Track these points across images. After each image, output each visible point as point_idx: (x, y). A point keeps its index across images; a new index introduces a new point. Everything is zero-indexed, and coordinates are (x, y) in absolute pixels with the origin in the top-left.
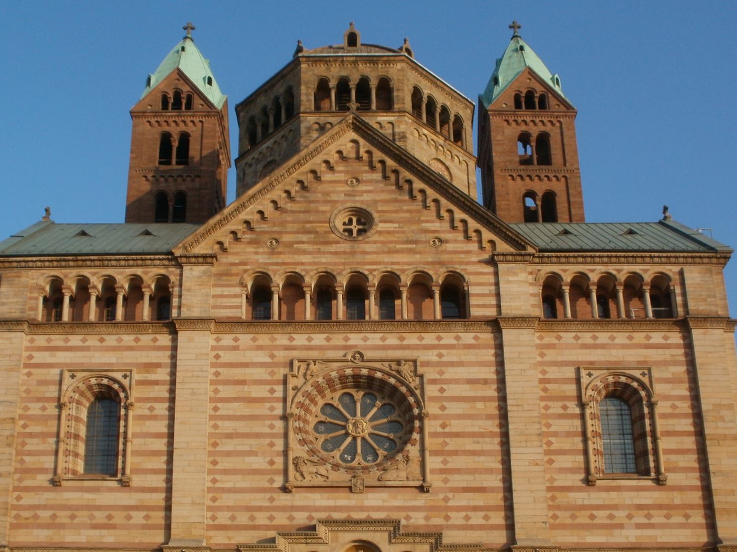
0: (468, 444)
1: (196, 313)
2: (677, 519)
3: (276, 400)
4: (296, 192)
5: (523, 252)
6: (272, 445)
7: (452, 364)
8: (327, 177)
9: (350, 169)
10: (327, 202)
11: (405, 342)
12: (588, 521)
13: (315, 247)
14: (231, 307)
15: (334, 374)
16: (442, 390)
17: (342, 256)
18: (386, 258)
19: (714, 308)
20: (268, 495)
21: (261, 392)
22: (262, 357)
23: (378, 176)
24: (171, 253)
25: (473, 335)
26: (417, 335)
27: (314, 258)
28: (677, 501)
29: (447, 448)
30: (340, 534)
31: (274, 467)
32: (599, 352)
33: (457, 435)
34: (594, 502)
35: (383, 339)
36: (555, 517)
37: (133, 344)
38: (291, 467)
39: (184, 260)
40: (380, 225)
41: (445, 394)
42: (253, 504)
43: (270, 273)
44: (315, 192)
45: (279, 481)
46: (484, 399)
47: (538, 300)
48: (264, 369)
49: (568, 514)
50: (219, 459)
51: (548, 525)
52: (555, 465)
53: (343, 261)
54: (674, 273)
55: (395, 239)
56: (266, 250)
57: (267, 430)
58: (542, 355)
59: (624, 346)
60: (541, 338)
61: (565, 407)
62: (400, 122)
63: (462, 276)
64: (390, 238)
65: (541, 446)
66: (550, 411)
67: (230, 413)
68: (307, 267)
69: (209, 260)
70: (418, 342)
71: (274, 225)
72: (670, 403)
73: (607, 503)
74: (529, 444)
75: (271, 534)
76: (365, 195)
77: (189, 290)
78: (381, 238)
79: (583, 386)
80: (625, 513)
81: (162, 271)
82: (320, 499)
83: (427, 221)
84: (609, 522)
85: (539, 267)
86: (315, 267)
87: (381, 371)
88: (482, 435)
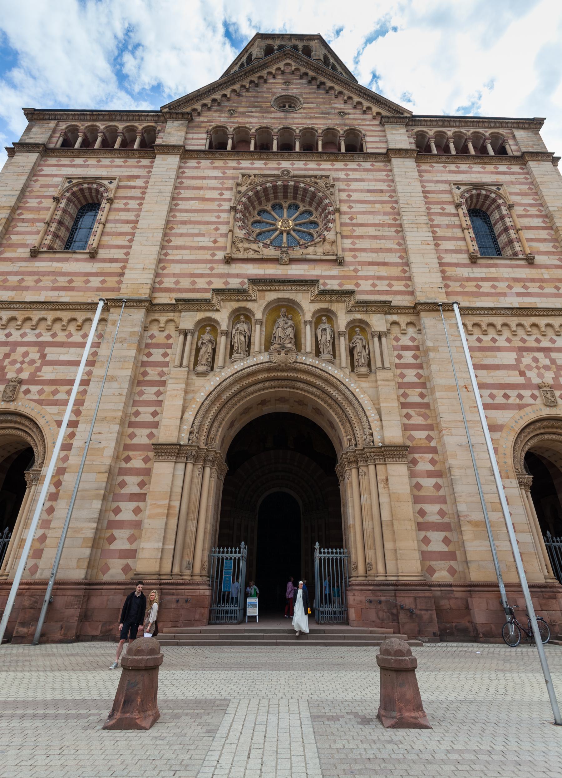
0: (371, 231)
3: (225, 200)
6: (217, 229)
7: (357, 180)
11: (321, 167)
12: (475, 290)
14: (198, 145)
15: (269, 185)
18: (308, 121)
20: (209, 266)
25: (370, 163)
26: (330, 163)
29: (354, 234)
30: (267, 294)
31: (217, 245)
32: (462, 175)
33: (362, 225)
39: (168, 116)
41: (351, 199)
42: (197, 272)
45: (220, 255)
46: (382, 202)
49: (458, 284)
52: (441, 247)
59: (479, 173)
64: (311, 111)
66: (431, 211)
67: (187, 207)
69: (186, 117)
70: (331, 167)
73: (488, 276)
74: (419, 230)
75: (208, 295)
78: (305, 111)
80: (507, 284)
88: (382, 225)
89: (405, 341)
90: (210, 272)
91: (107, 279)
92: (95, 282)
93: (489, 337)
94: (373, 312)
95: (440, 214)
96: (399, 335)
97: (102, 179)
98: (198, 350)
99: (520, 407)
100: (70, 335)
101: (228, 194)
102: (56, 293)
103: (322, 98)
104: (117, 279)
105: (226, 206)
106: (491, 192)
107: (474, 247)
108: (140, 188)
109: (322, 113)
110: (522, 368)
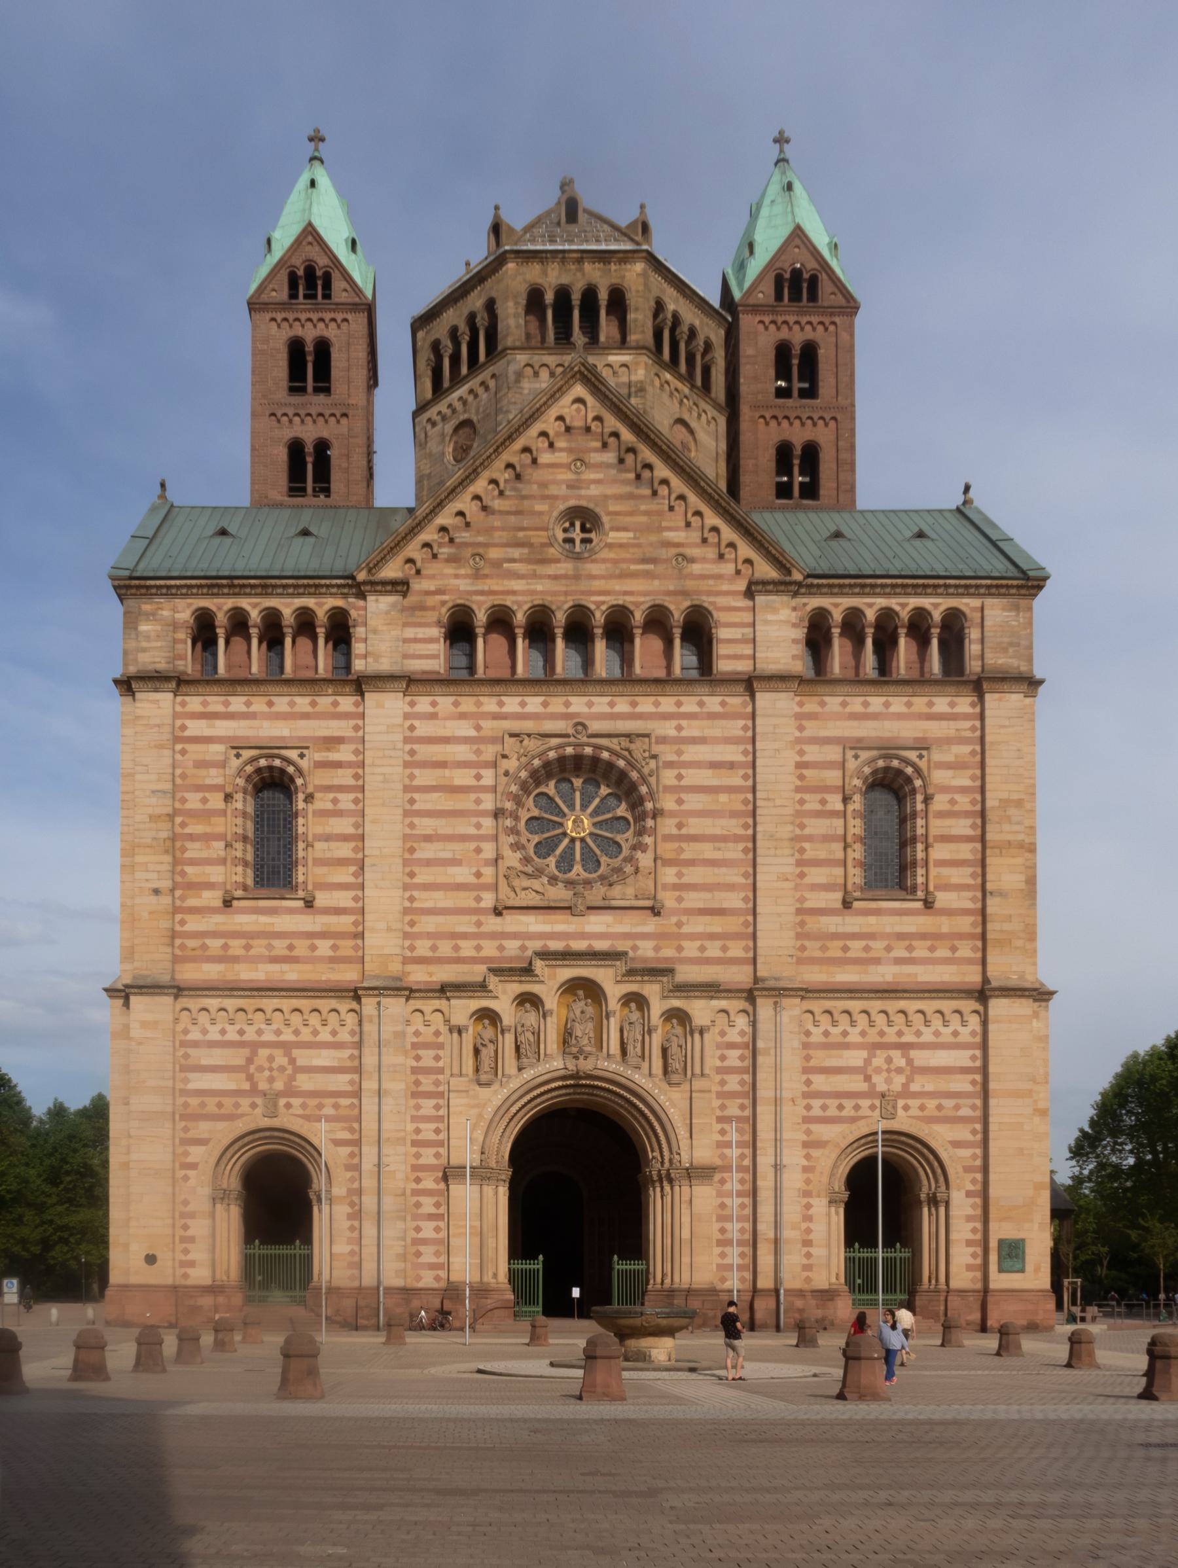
0: (707, 851)
1: (385, 665)
2: (943, 953)
3: (484, 789)
4: (506, 481)
5: (788, 579)
7: (694, 741)
8: (545, 458)
9: (573, 445)
10: (545, 498)
11: (639, 709)
12: (839, 954)
13: (531, 567)
14: (427, 657)
16: (680, 777)
17: (564, 582)
18: (617, 586)
19: (1014, 662)
20: (474, 918)
21: (463, 778)
22: (465, 729)
23: (610, 457)
24: (353, 578)
25: (720, 699)
26: (652, 699)
27: (528, 584)
28: (945, 929)
29: (683, 856)
30: (558, 970)
32: (870, 724)
34: (849, 929)
35: (612, 704)
36: (803, 948)
37: (309, 709)
38: (501, 879)
39: (368, 588)
40: (612, 534)
41: (683, 783)
43: (474, 607)
44: (529, 482)
45: (488, 900)
46: (730, 790)
47: (800, 649)
48: (468, 746)
49: (819, 944)
50: (416, 870)
51: (794, 959)
52: (808, 880)
53: (564, 589)
54: (974, 609)
55: (628, 556)
56: (469, 571)
57: (472, 831)
58: (801, 728)
59: (899, 717)
60: (801, 704)
61: (823, 802)
62: (637, 364)
63: (710, 613)
64: (624, 554)
65: (793, 855)
67: (429, 806)
68: (520, 598)
69: (399, 588)
70: (653, 710)
71: (479, 532)
72: (947, 797)
73: (865, 930)
74: (779, 852)
76: (592, 487)
77: (375, 632)
78: (612, 555)
79: (848, 773)
80: (884, 943)
81: (339, 602)
82: (533, 923)
83: (669, 529)
84: (864, 955)
85: (805, 600)
86: (528, 598)
87: (608, 749)
88: (724, 839)
89: (733, 1036)
90: (476, 930)
91: (340, 943)
92: (324, 947)
93: (839, 1029)
94: (696, 997)
95: (819, 814)
96: (727, 1029)
97: (286, 748)
98: (477, 1052)
99: (853, 1120)
100: (315, 1033)
101: (488, 777)
102: (275, 967)
103: (647, 513)
104: (351, 943)
105: (488, 803)
106: (908, 762)
107: (856, 876)
108: (349, 765)
109: (645, 561)
110: (870, 1071)
